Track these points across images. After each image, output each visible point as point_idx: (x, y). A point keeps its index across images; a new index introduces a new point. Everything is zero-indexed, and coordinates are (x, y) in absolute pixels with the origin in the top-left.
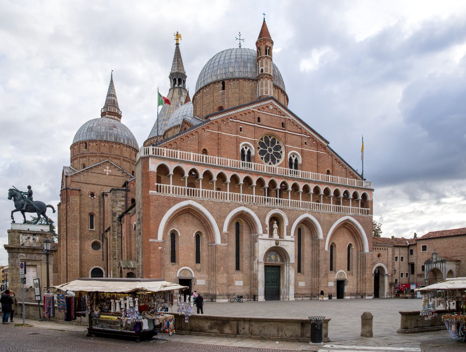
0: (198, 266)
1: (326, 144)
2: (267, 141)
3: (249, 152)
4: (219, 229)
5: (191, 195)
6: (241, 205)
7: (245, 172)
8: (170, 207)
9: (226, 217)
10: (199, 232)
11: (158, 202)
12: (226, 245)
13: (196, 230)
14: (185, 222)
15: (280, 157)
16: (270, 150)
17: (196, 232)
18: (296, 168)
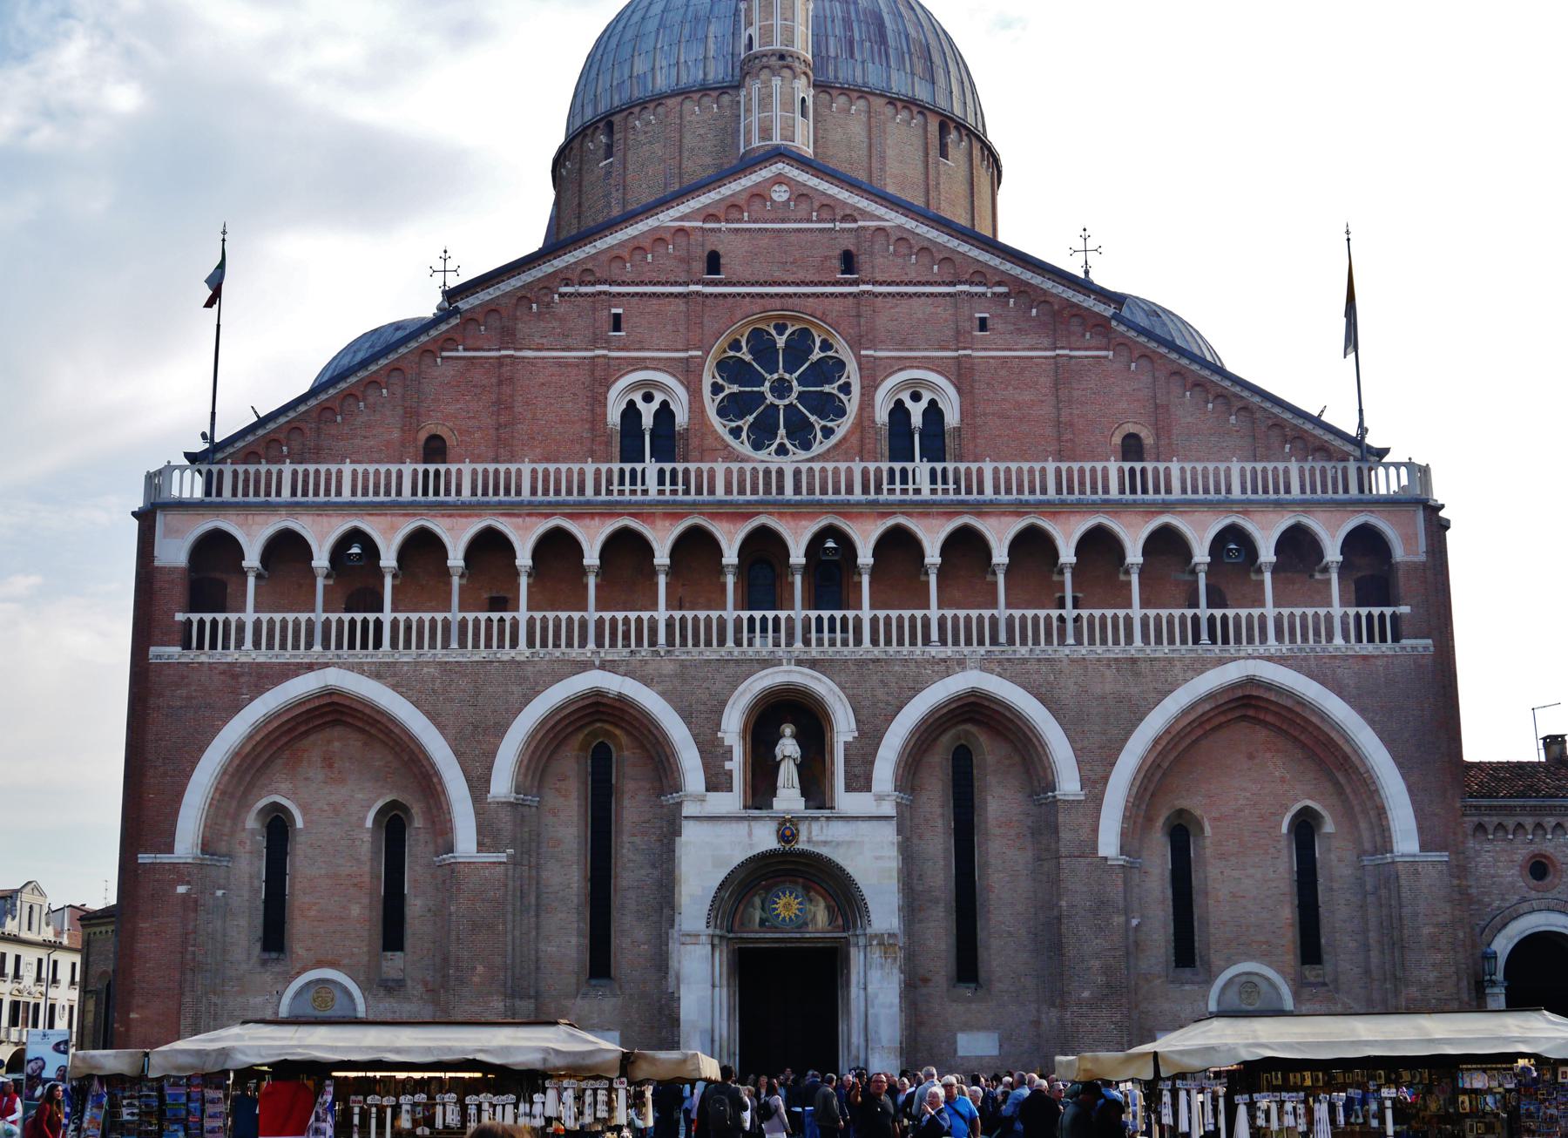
0: (394, 964)
1: (1108, 311)
2: (762, 346)
3: (665, 413)
4: (470, 787)
5: (339, 646)
6: (583, 666)
7: (608, 510)
8: (237, 708)
9: (508, 726)
10: (393, 805)
11: (184, 692)
12: (502, 857)
13: (379, 796)
14: (331, 766)
15: (841, 412)
16: (781, 389)
17: (380, 804)
18: (934, 452)
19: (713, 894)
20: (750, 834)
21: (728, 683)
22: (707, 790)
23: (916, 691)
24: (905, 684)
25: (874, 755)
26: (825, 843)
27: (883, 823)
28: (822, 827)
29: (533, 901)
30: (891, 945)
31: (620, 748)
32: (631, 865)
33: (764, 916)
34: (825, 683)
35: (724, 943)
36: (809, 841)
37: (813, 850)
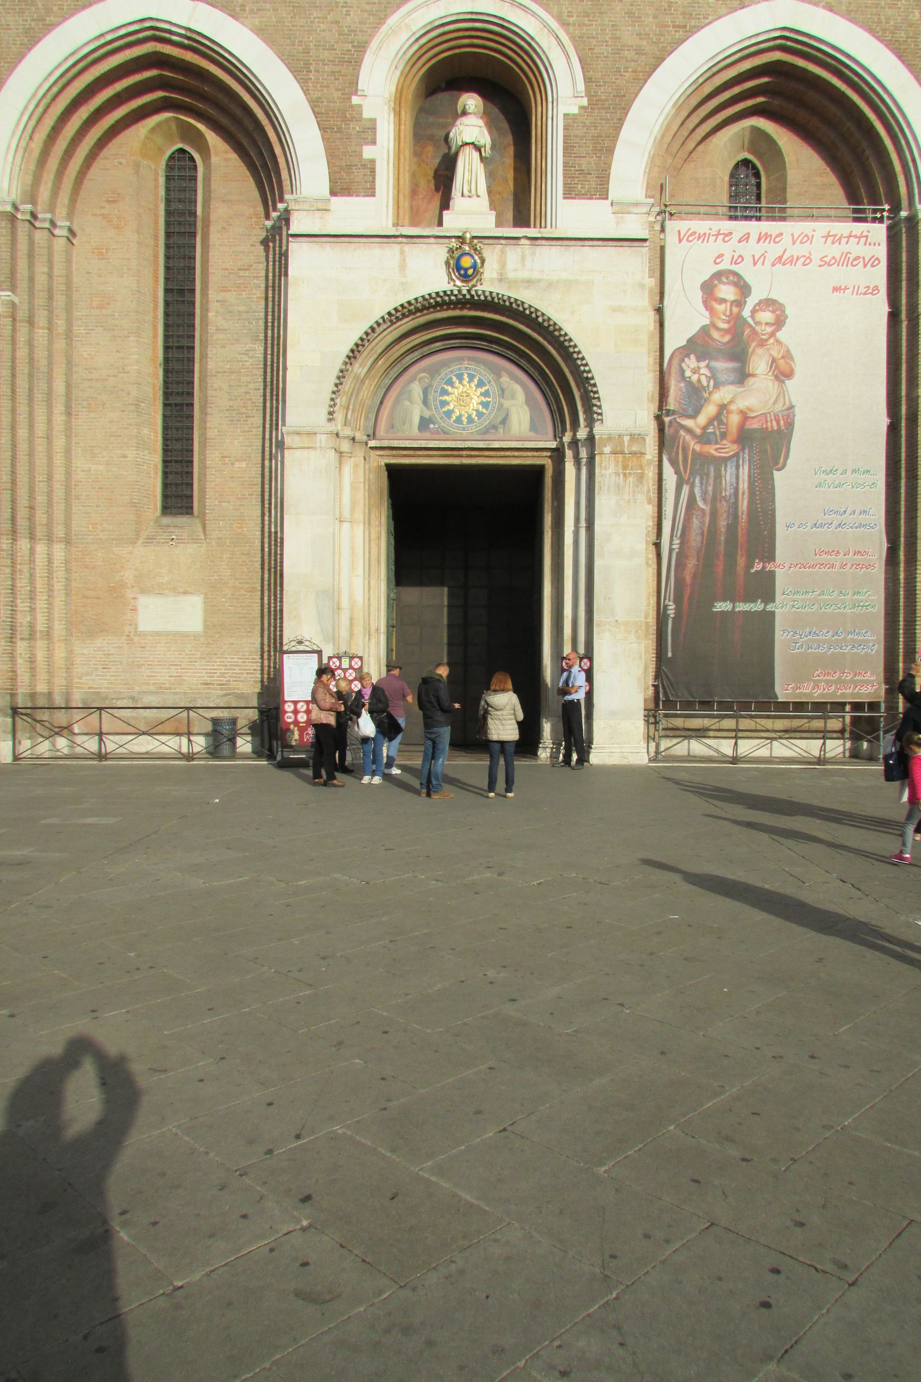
19: (339, 365)
20: (403, 267)
21: (371, 13)
22: (333, 193)
23: (689, 31)
24: (668, 20)
25: (614, 137)
26: (529, 283)
27: (626, 252)
28: (523, 258)
29: (59, 387)
30: (633, 453)
31: (204, 150)
32: (222, 336)
33: (427, 414)
34: (534, 14)
35: (360, 452)
36: (500, 280)
37: (507, 293)
